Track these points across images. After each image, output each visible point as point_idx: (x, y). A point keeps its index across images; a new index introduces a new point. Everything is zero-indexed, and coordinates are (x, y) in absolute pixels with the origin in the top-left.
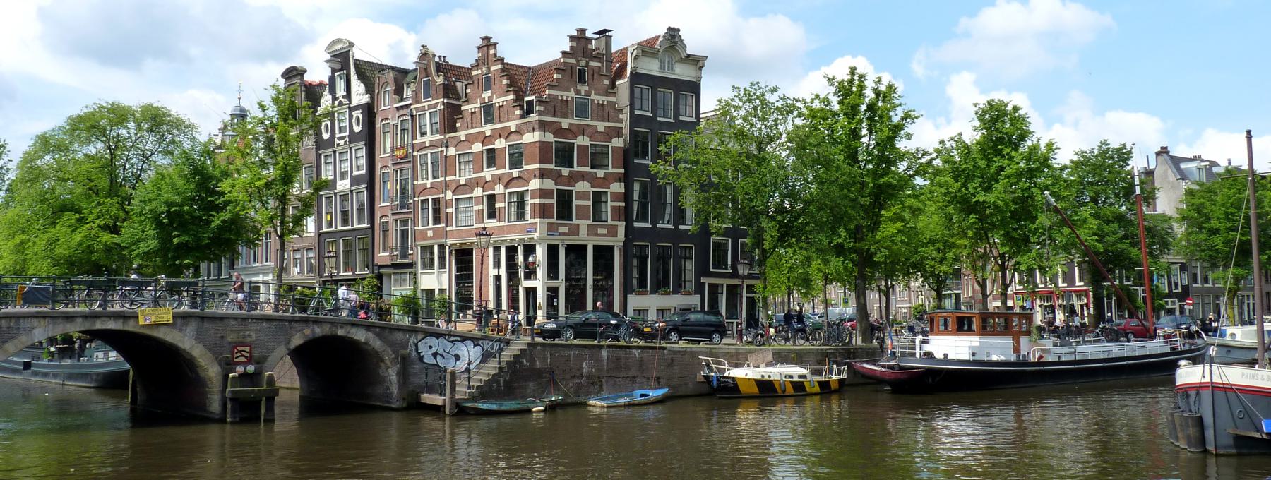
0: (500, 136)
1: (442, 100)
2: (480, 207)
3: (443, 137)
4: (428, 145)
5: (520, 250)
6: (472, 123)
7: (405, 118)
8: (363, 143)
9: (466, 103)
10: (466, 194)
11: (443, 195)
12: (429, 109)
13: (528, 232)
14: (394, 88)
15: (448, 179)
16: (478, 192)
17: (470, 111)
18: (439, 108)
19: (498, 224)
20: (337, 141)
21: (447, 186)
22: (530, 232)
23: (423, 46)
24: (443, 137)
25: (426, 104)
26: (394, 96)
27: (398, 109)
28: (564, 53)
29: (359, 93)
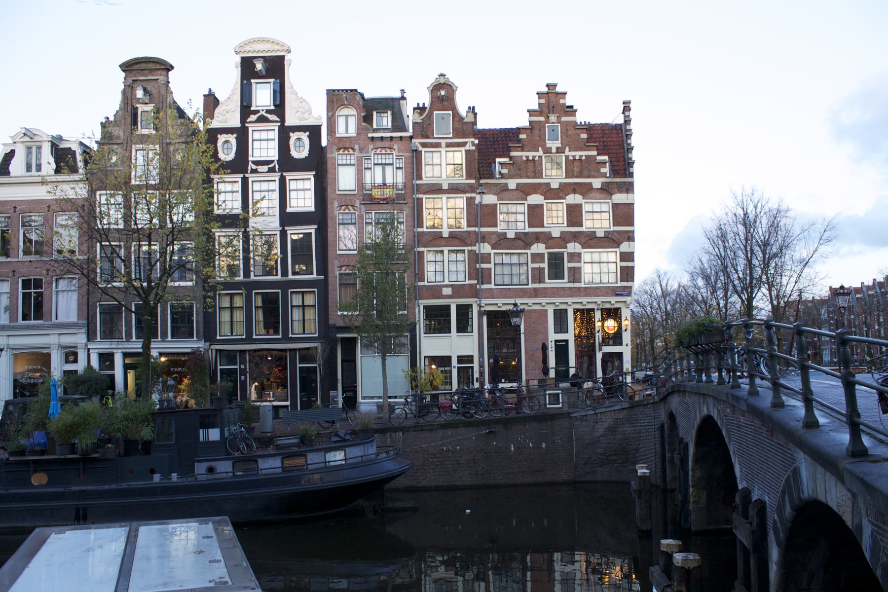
0: (574, 192)
1: (473, 140)
2: (542, 265)
3: (473, 181)
4: (445, 187)
5: (598, 315)
6: (527, 172)
7: (383, 152)
8: (314, 173)
9: (520, 149)
10: (516, 249)
11: (474, 248)
12: (447, 146)
13: (617, 295)
14: (363, 114)
15: (483, 229)
16: (539, 248)
17: (525, 158)
18: (467, 147)
19: (571, 285)
20: (251, 166)
21: (484, 238)
22: (622, 295)
23: (442, 75)
24: (473, 181)
25: (443, 142)
26: (364, 124)
27: (373, 139)
28: (531, 112)
29: (301, 110)
